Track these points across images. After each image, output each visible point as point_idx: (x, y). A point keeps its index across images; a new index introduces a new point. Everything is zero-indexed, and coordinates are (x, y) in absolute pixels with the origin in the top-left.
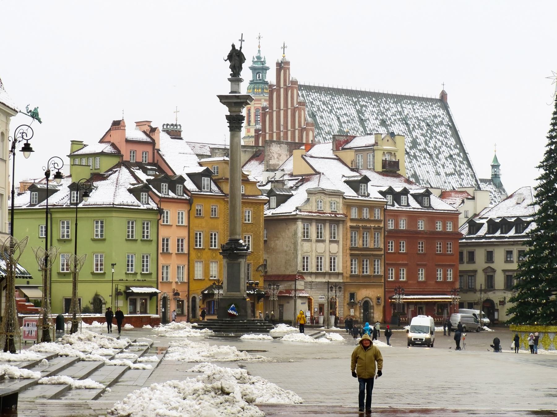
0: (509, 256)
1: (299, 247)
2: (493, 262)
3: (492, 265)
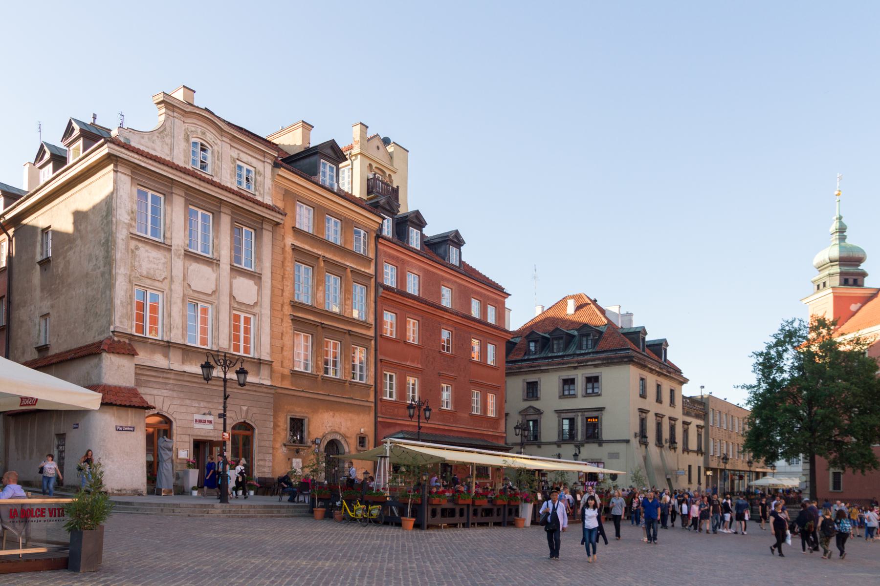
0: (566, 387)
2: (537, 399)
3: (536, 404)
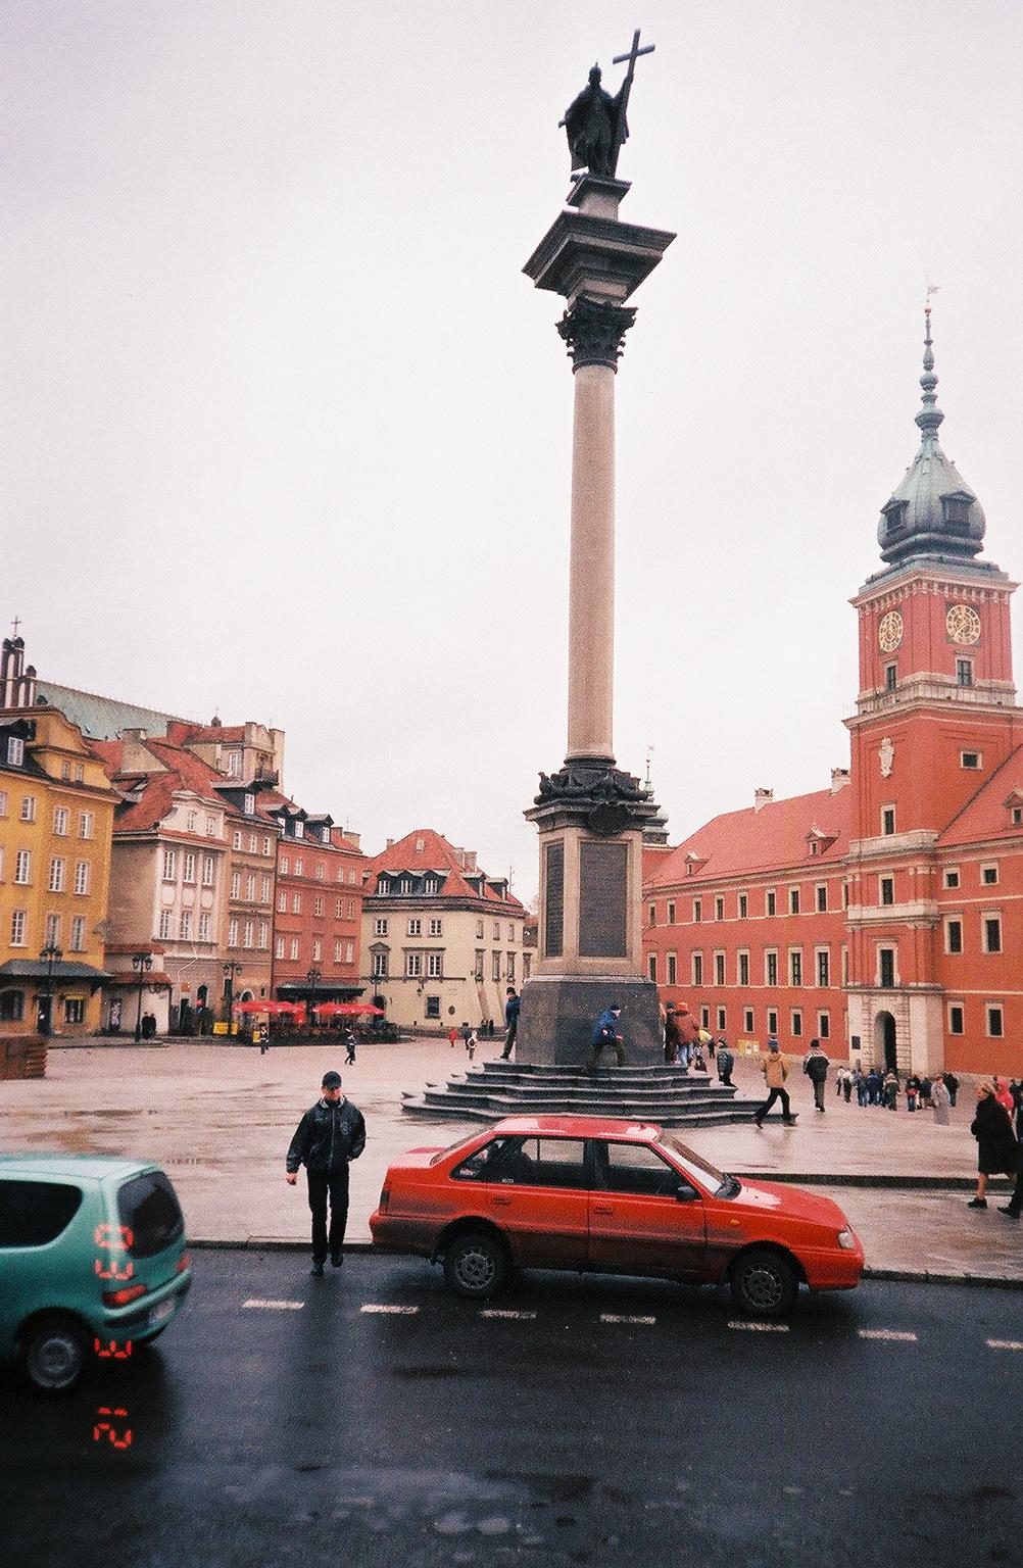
1: (157, 894)
3: (383, 940)
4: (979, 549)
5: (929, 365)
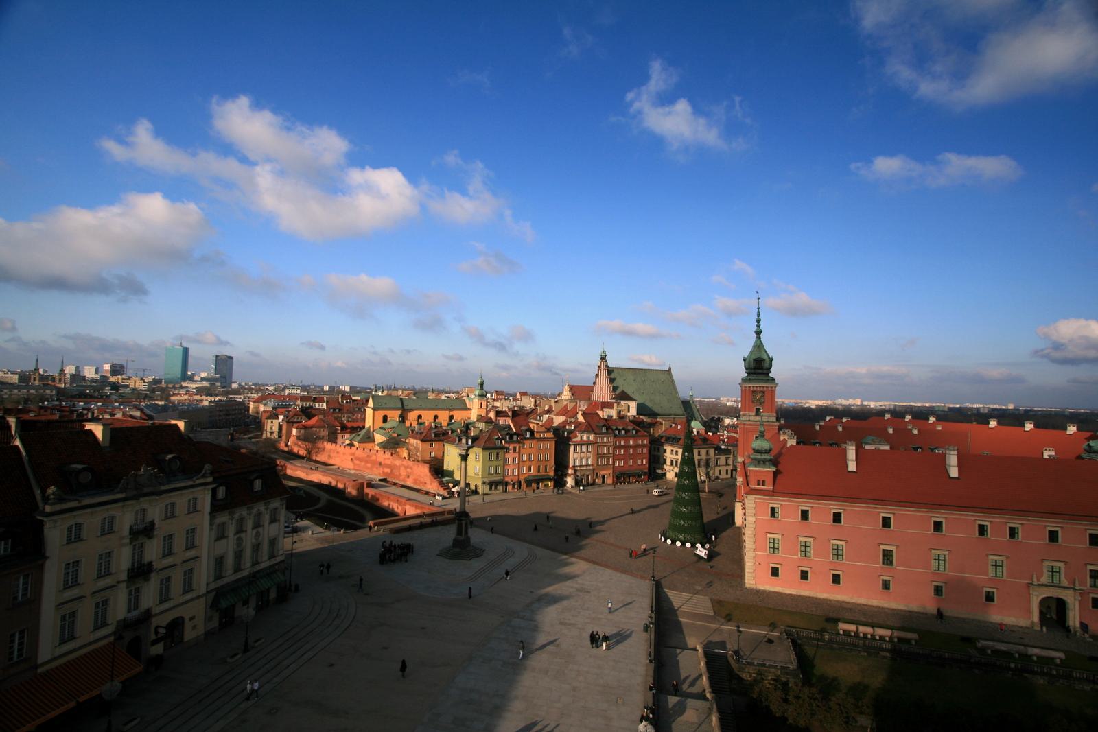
4: (770, 372)
5: (758, 315)
